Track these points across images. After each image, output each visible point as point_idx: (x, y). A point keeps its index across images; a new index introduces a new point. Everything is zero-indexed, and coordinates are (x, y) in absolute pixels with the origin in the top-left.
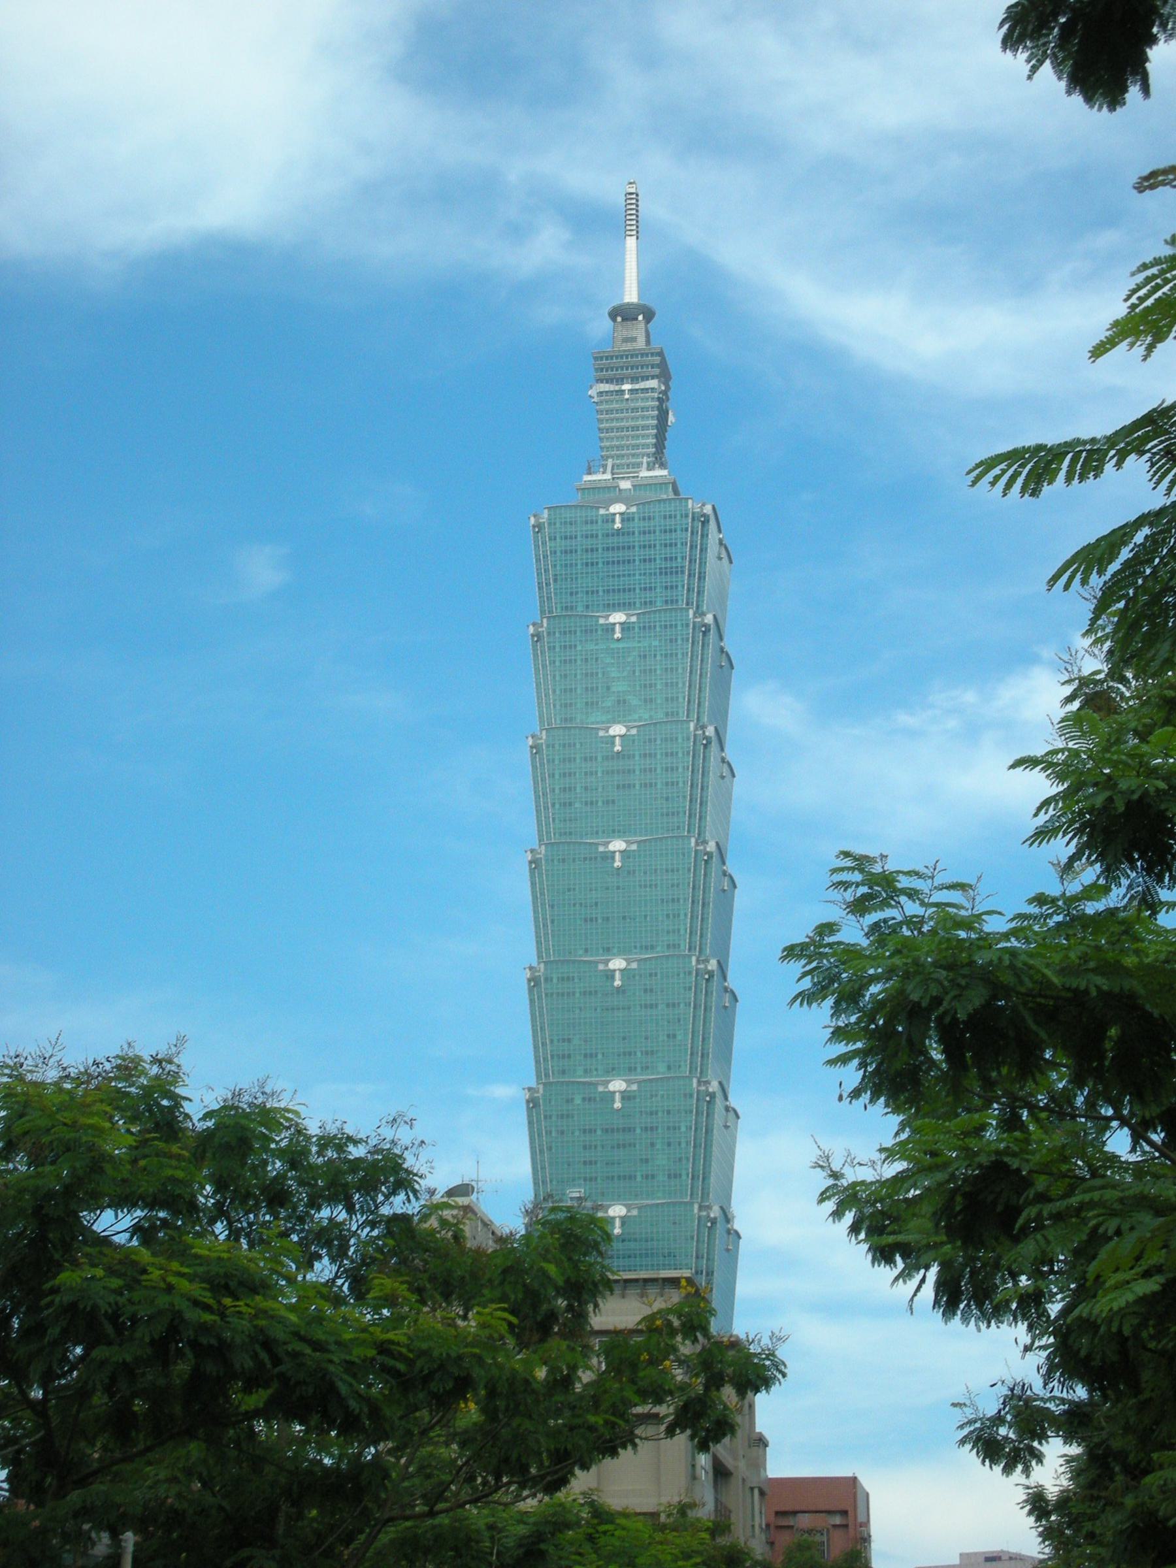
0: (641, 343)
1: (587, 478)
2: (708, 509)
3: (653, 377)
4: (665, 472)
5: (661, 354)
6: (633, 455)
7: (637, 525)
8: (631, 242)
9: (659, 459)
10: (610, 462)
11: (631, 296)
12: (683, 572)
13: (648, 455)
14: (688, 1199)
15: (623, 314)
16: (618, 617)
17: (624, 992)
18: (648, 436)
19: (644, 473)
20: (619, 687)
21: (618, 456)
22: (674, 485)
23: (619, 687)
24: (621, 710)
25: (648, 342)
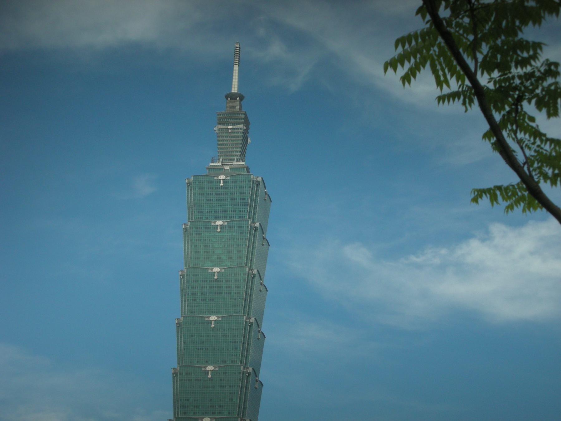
1: (212, 164)
4: (244, 163)
5: (245, 114)
9: (242, 157)
10: (221, 158)
11: (235, 90)
12: (247, 205)
15: (231, 97)
16: (219, 223)
17: (212, 380)
19: (235, 163)
25: (240, 109)
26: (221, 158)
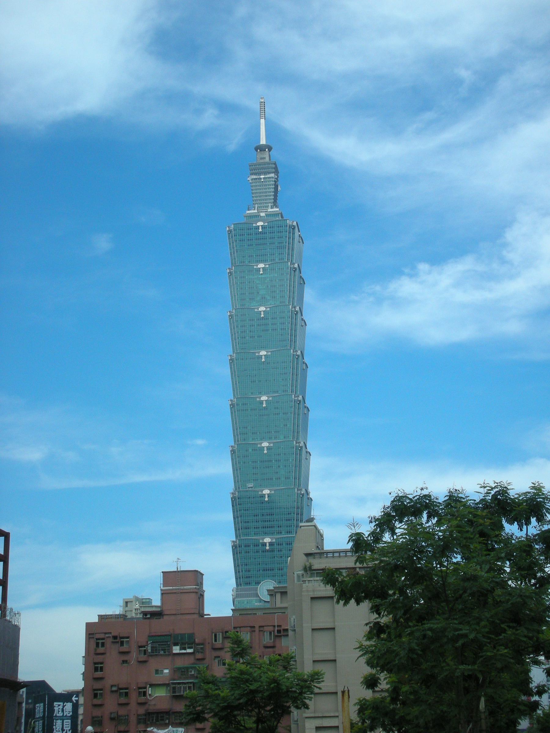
0: (267, 160)
2: (295, 224)
3: (272, 173)
4: (278, 209)
5: (275, 164)
6: (265, 203)
7: (268, 230)
8: (263, 121)
9: (275, 204)
10: (256, 206)
11: (263, 142)
15: (261, 149)
16: (261, 266)
18: (271, 195)
19: (270, 210)
20: (262, 292)
22: (281, 214)
24: (263, 301)
25: (270, 160)
26: (256, 206)
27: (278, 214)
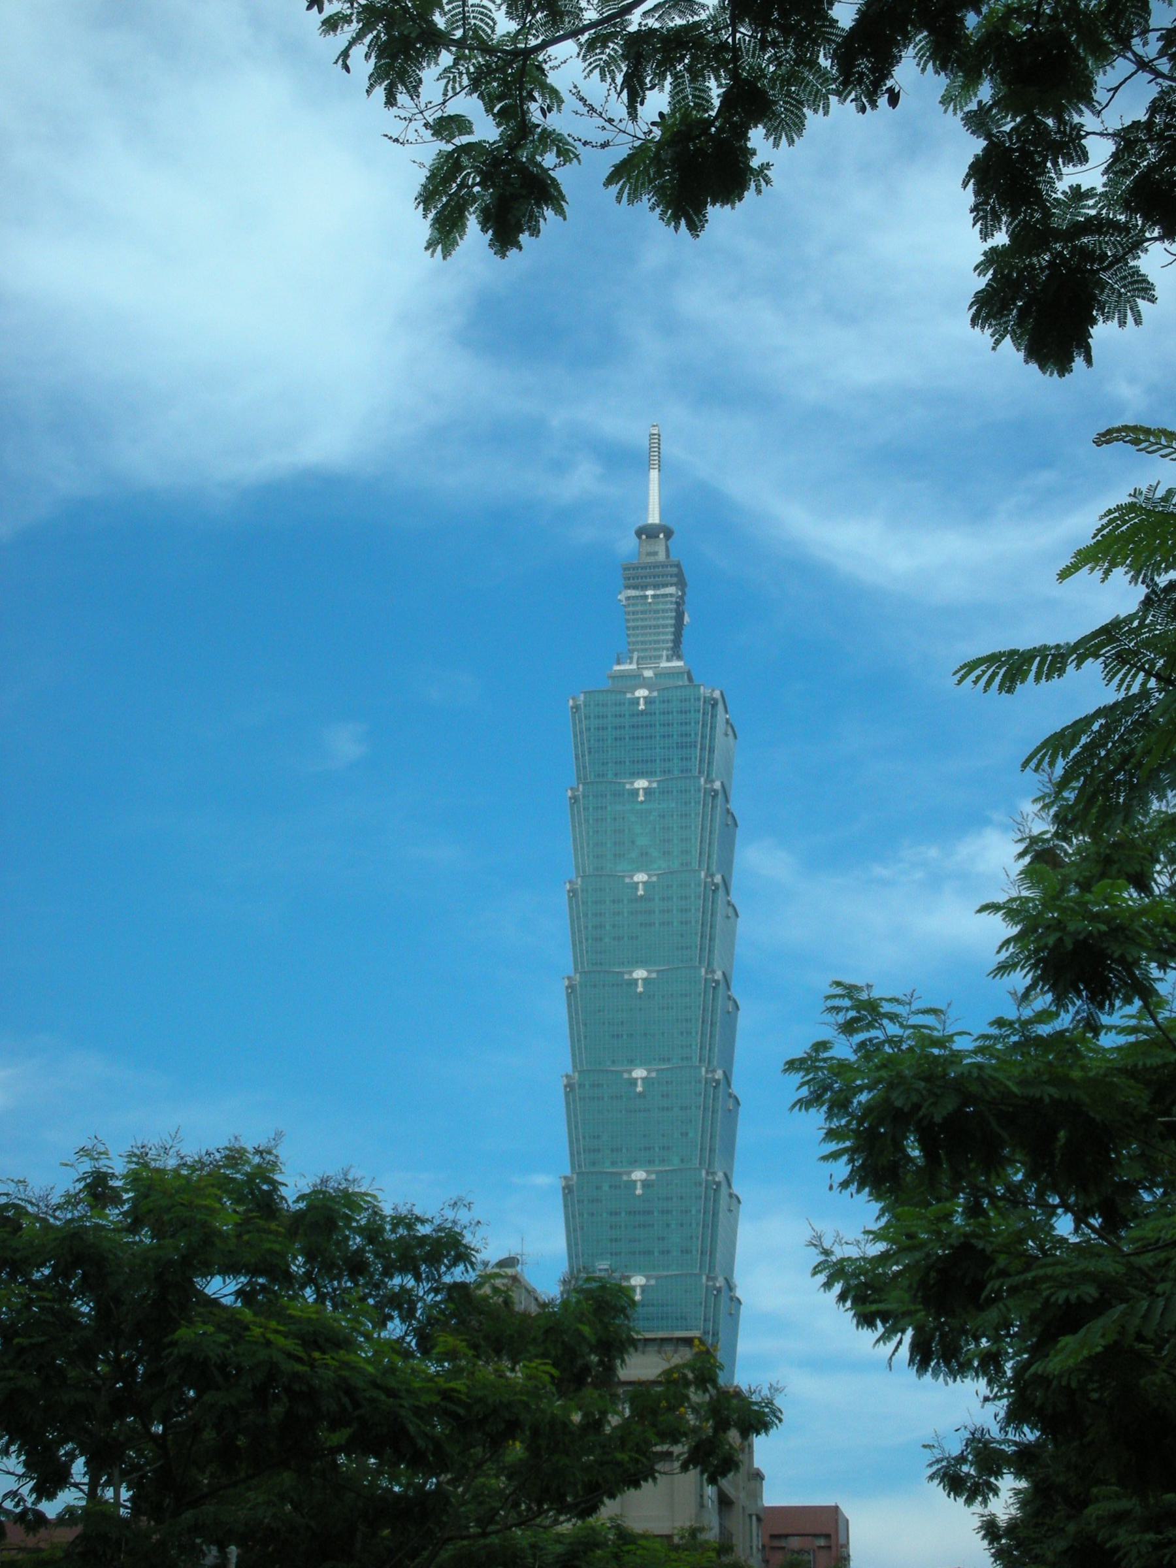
0: (662, 557)
2: (717, 694)
3: (672, 585)
4: (681, 664)
5: (678, 566)
6: (655, 649)
8: (654, 474)
9: (676, 653)
10: (635, 655)
11: (654, 518)
12: (695, 747)
13: (667, 649)
14: (697, 1271)
15: (647, 533)
16: (641, 783)
19: (664, 664)
20: (642, 841)
21: (643, 650)
23: (642, 841)
25: (668, 556)
26: (635, 655)
27: (682, 673)
